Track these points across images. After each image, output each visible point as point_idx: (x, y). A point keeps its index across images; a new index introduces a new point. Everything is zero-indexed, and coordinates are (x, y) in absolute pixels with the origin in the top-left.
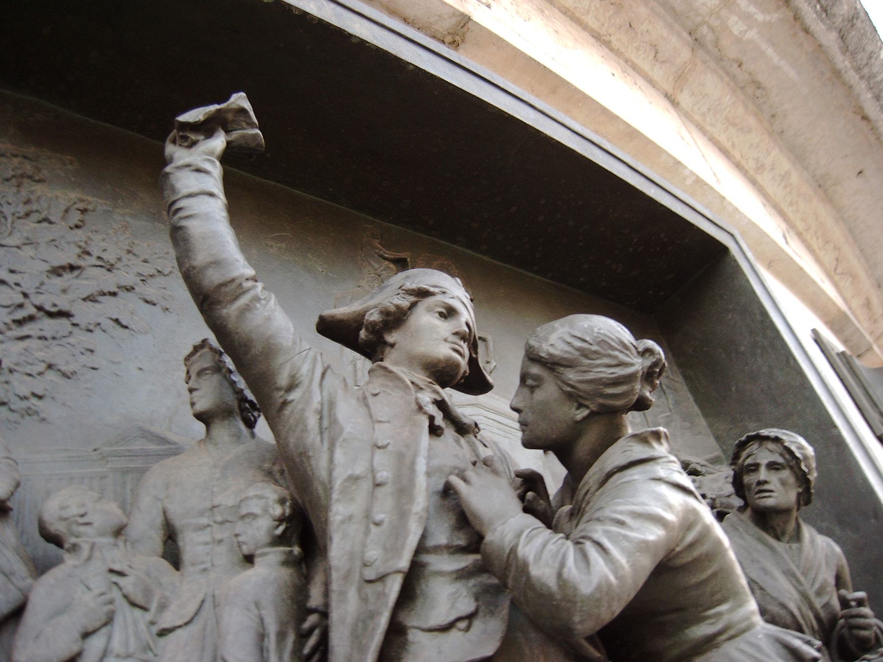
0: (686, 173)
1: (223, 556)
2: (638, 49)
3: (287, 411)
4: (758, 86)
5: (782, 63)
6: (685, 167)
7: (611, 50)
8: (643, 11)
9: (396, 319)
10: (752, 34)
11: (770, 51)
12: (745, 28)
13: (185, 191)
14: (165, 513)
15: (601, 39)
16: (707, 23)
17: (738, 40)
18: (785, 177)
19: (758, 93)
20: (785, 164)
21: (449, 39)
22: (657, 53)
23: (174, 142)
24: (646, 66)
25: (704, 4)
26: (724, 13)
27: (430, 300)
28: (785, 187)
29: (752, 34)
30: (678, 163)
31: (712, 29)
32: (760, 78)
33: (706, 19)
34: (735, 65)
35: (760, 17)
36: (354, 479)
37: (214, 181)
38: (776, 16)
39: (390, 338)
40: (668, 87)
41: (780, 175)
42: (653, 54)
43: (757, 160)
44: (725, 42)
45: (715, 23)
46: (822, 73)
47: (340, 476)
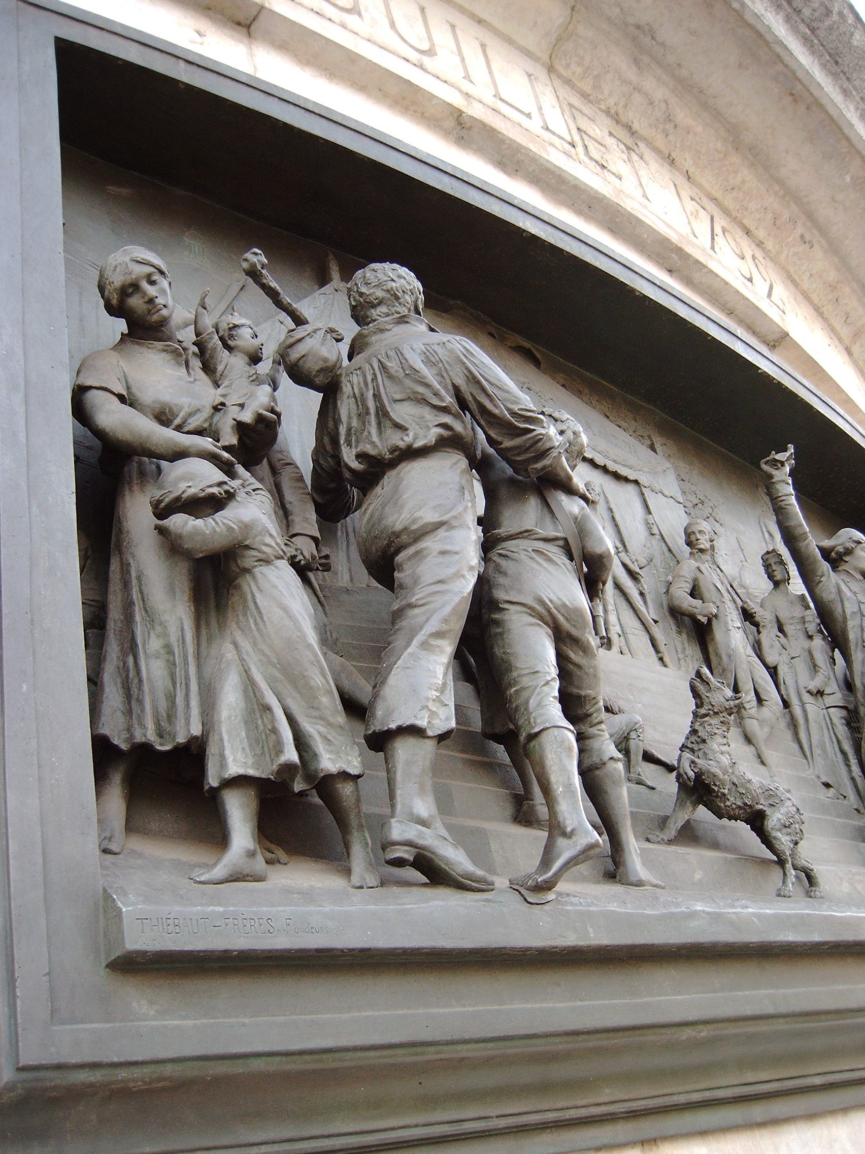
1: (802, 636)
3: (821, 585)
7: (822, 318)
8: (847, 290)
9: (849, 552)
13: (785, 492)
14: (777, 617)
15: (819, 311)
21: (772, 343)
23: (766, 463)
24: (838, 327)
27: (861, 545)
36: (854, 613)
37: (791, 489)
39: (846, 558)
40: (847, 341)
47: (848, 612)
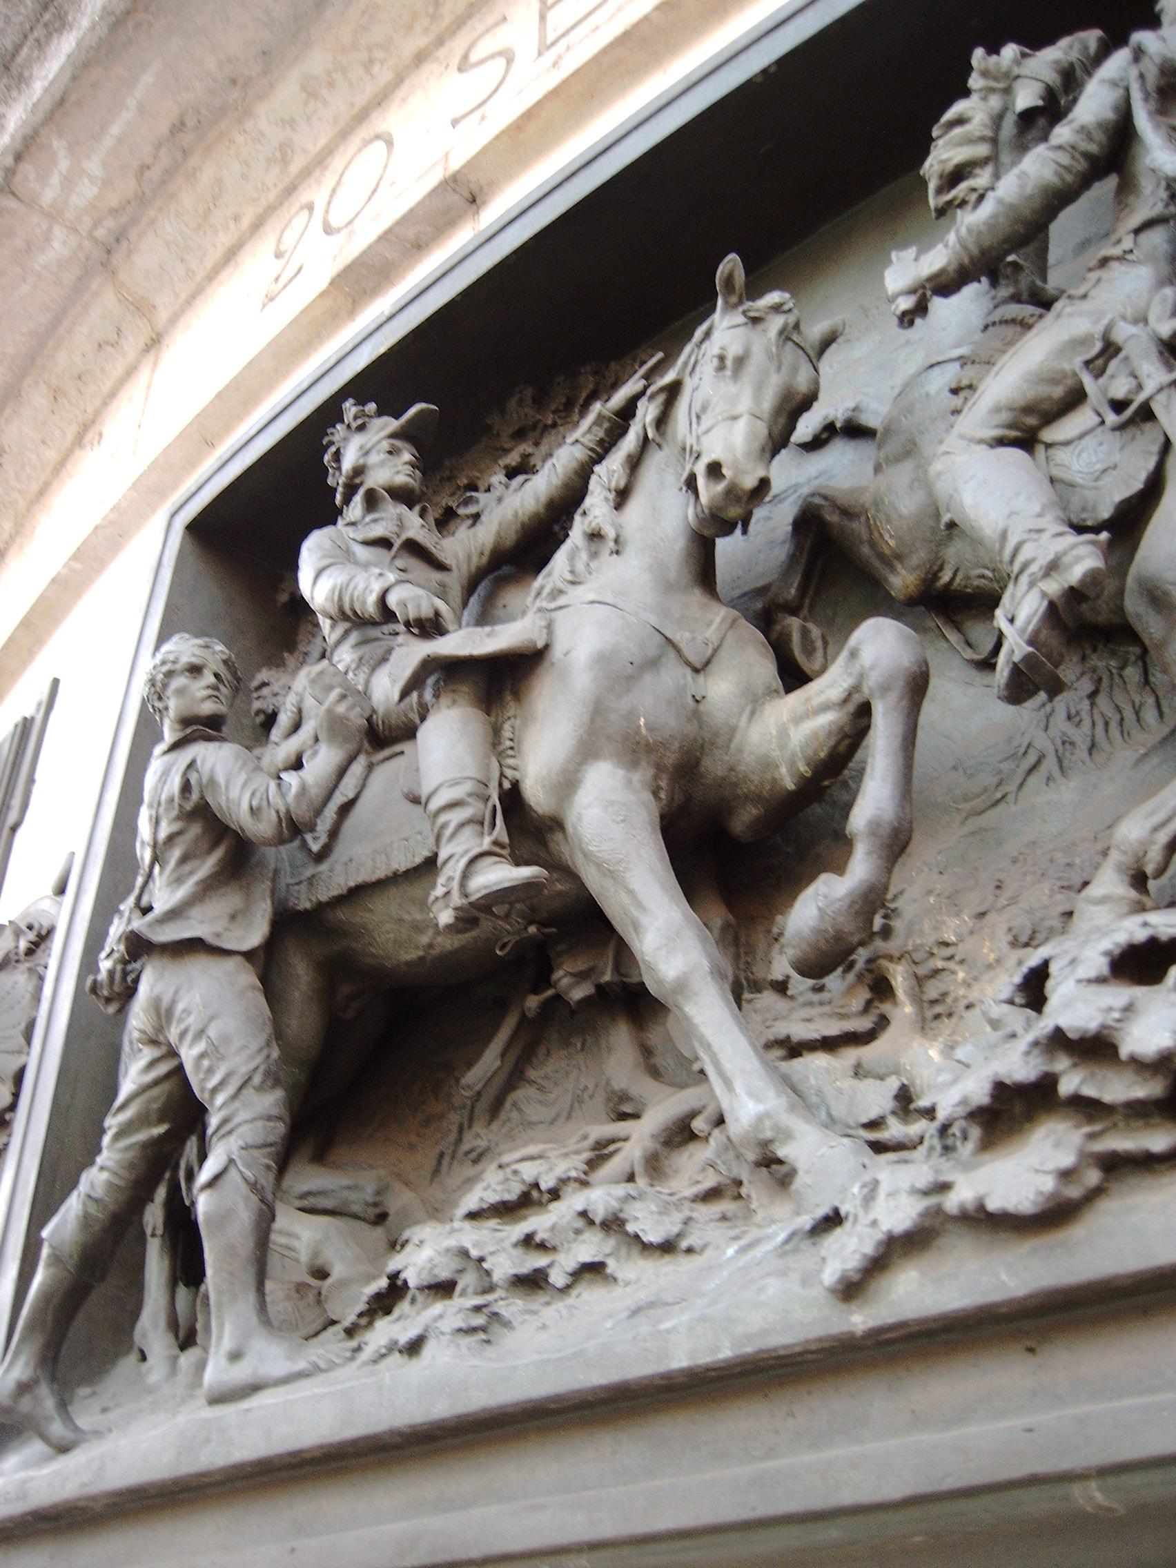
0: (65, 571)
2: (103, 370)
4: (179, 126)
5: (131, 102)
6: (59, 574)
10: (93, 166)
11: (115, 129)
12: (86, 181)
16: (90, 233)
17: (107, 183)
18: (310, 92)
19: (191, 122)
20: (287, 93)
22: (108, 343)
25: (64, 243)
26: (70, 215)
28: (331, 85)
29: (93, 166)
30: (54, 580)
31: (96, 225)
32: (163, 127)
33: (84, 234)
34: (148, 174)
35: (64, 164)
38: (55, 143)
41: (306, 103)
42: (109, 349)
43: (270, 161)
44: (113, 200)
45: (87, 221)
46: (137, 26)
